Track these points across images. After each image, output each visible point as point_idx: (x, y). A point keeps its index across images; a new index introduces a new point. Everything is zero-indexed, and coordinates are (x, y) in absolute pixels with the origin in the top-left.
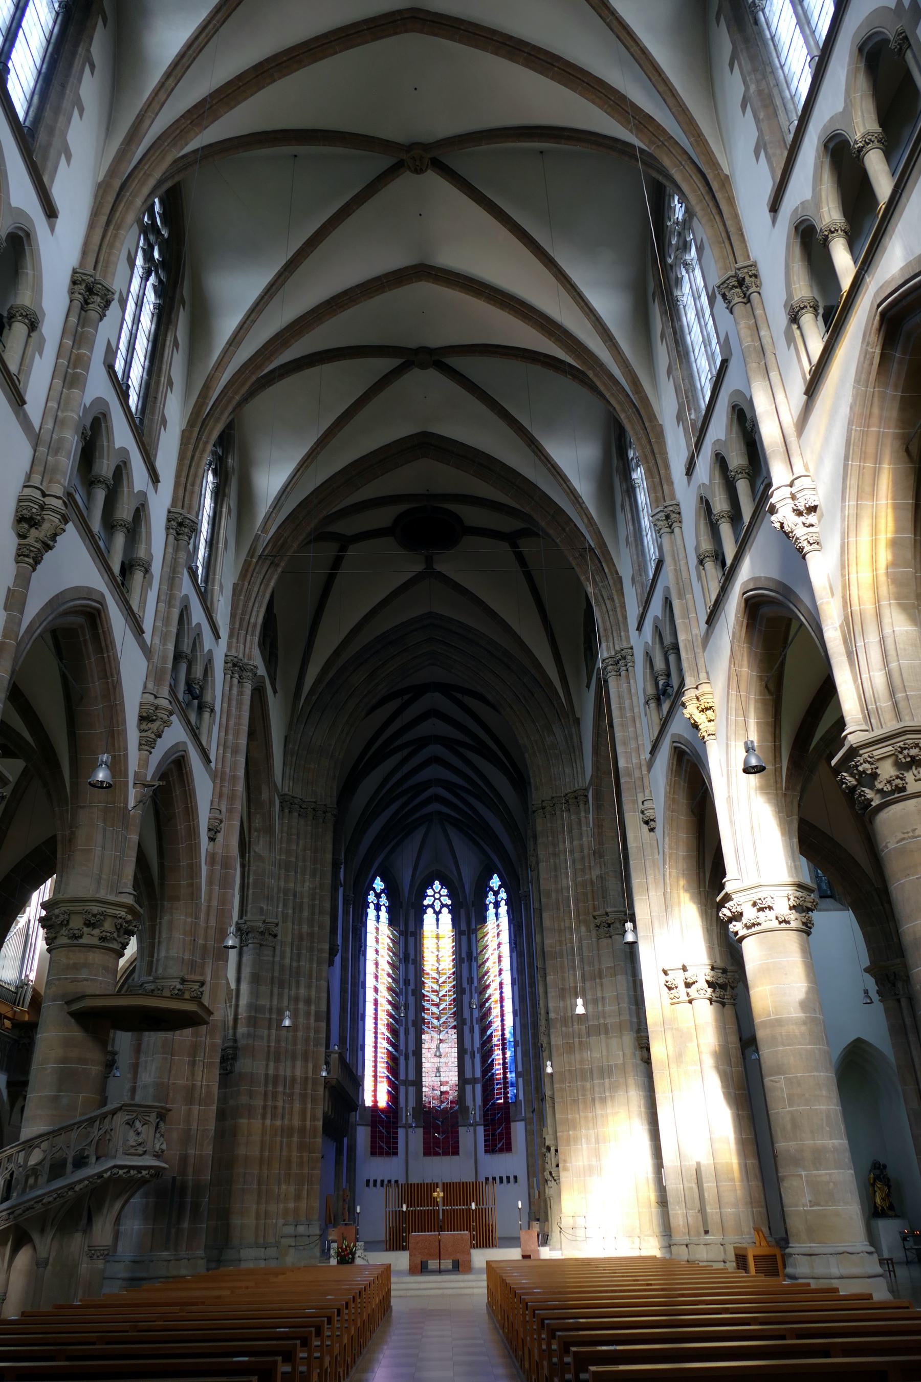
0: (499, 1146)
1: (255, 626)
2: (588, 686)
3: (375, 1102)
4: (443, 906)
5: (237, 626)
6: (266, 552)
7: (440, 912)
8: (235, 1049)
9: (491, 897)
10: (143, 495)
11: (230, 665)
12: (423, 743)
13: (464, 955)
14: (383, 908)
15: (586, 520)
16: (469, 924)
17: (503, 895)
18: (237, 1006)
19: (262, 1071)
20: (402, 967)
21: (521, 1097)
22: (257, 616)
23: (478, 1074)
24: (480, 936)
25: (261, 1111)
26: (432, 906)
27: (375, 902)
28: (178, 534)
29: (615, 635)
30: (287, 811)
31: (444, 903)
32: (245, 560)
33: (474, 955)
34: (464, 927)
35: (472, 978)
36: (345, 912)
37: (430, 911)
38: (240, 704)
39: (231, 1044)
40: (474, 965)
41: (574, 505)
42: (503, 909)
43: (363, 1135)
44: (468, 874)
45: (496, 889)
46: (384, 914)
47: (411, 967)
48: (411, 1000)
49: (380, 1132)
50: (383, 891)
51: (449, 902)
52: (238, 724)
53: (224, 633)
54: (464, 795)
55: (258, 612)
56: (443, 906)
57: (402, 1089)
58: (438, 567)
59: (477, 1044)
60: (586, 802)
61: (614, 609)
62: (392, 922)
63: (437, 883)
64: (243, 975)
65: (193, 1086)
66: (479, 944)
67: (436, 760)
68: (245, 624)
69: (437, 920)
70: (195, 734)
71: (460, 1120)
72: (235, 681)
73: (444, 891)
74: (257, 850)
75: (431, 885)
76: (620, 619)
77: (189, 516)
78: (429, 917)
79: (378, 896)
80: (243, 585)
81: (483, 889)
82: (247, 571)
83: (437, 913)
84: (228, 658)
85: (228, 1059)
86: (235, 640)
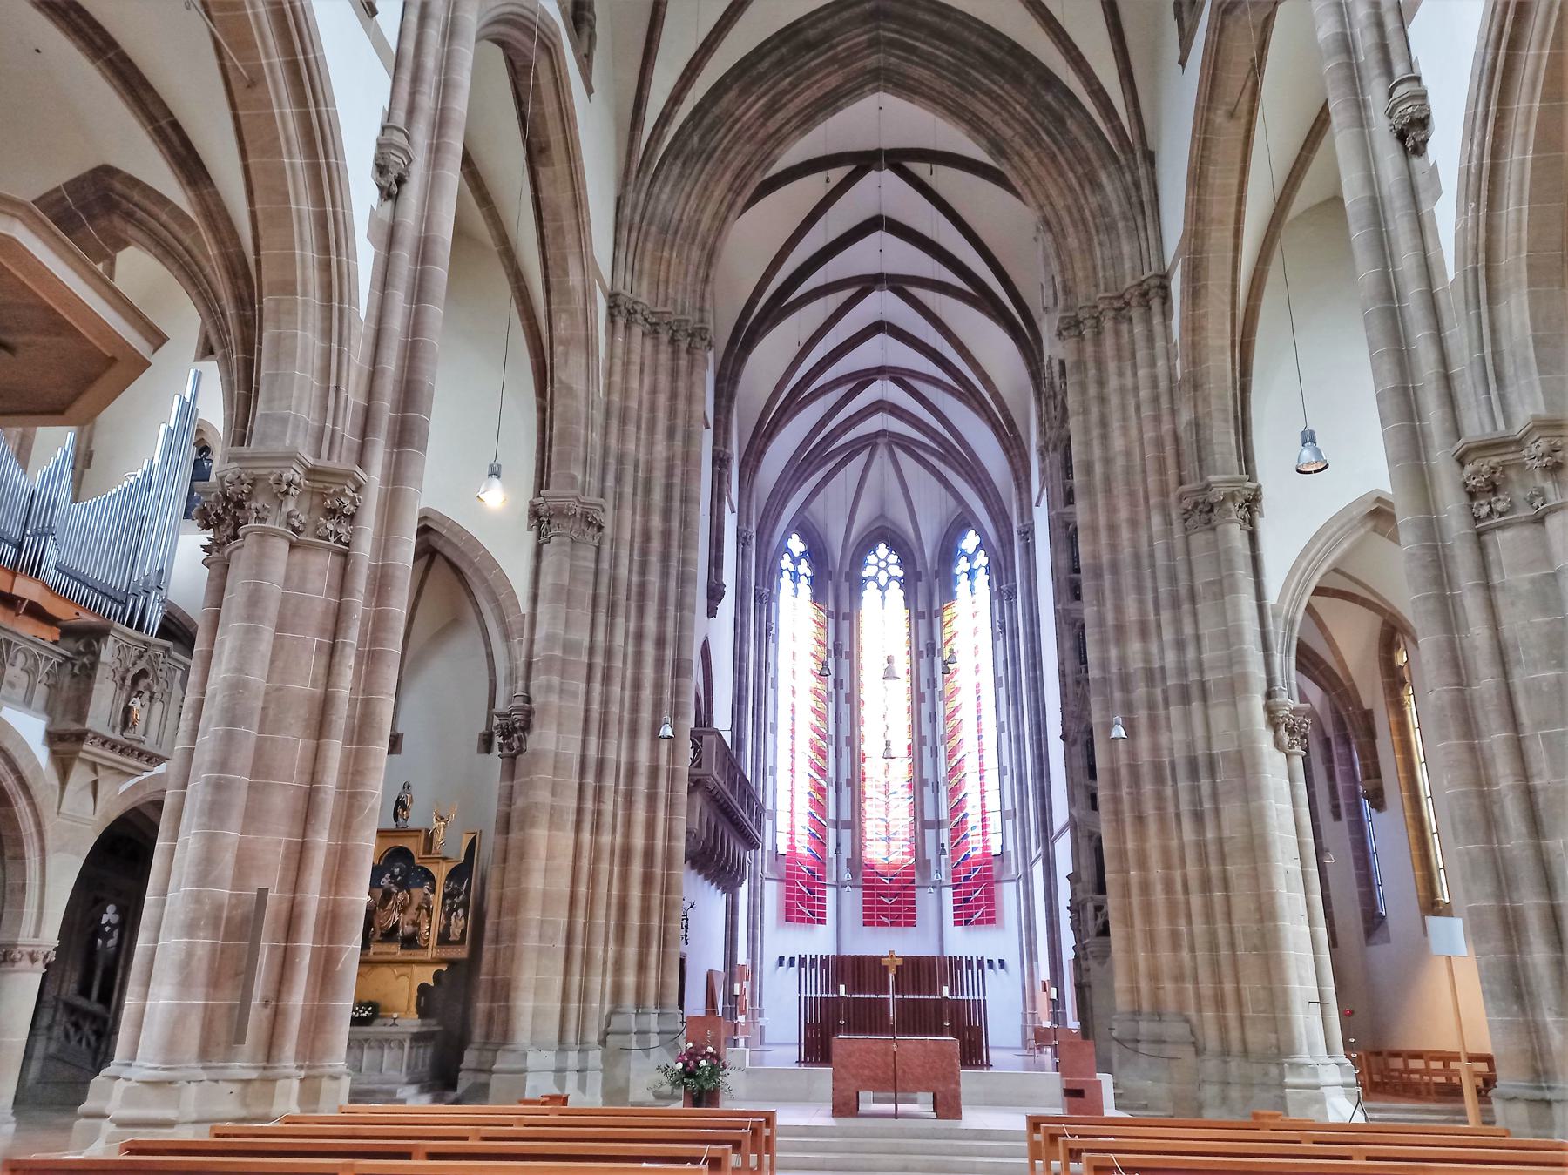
0: (976, 916)
2: (1182, 62)
3: (792, 847)
4: (890, 578)
7: (887, 587)
8: (529, 713)
9: (963, 565)
12: (864, 379)
13: (922, 647)
14: (803, 579)
17: (982, 559)
18: (531, 642)
19: (575, 751)
20: (831, 662)
21: (1010, 847)
23: (944, 814)
24: (946, 619)
26: (875, 578)
27: (792, 569)
30: (621, 321)
31: (893, 574)
33: (938, 646)
34: (922, 608)
35: (935, 680)
37: (871, 586)
39: (519, 703)
40: (938, 662)
42: (982, 579)
43: (772, 894)
45: (970, 551)
46: (805, 589)
47: (845, 663)
49: (800, 890)
51: (901, 573)
54: (922, 453)
57: (832, 832)
59: (943, 773)
60: (1166, 298)
62: (817, 598)
63: (882, 549)
64: (541, 592)
65: (550, 828)
66: (947, 630)
69: (883, 598)
71: (917, 878)
73: (893, 558)
78: (870, 594)
79: (795, 561)
81: (948, 553)
85: (515, 730)
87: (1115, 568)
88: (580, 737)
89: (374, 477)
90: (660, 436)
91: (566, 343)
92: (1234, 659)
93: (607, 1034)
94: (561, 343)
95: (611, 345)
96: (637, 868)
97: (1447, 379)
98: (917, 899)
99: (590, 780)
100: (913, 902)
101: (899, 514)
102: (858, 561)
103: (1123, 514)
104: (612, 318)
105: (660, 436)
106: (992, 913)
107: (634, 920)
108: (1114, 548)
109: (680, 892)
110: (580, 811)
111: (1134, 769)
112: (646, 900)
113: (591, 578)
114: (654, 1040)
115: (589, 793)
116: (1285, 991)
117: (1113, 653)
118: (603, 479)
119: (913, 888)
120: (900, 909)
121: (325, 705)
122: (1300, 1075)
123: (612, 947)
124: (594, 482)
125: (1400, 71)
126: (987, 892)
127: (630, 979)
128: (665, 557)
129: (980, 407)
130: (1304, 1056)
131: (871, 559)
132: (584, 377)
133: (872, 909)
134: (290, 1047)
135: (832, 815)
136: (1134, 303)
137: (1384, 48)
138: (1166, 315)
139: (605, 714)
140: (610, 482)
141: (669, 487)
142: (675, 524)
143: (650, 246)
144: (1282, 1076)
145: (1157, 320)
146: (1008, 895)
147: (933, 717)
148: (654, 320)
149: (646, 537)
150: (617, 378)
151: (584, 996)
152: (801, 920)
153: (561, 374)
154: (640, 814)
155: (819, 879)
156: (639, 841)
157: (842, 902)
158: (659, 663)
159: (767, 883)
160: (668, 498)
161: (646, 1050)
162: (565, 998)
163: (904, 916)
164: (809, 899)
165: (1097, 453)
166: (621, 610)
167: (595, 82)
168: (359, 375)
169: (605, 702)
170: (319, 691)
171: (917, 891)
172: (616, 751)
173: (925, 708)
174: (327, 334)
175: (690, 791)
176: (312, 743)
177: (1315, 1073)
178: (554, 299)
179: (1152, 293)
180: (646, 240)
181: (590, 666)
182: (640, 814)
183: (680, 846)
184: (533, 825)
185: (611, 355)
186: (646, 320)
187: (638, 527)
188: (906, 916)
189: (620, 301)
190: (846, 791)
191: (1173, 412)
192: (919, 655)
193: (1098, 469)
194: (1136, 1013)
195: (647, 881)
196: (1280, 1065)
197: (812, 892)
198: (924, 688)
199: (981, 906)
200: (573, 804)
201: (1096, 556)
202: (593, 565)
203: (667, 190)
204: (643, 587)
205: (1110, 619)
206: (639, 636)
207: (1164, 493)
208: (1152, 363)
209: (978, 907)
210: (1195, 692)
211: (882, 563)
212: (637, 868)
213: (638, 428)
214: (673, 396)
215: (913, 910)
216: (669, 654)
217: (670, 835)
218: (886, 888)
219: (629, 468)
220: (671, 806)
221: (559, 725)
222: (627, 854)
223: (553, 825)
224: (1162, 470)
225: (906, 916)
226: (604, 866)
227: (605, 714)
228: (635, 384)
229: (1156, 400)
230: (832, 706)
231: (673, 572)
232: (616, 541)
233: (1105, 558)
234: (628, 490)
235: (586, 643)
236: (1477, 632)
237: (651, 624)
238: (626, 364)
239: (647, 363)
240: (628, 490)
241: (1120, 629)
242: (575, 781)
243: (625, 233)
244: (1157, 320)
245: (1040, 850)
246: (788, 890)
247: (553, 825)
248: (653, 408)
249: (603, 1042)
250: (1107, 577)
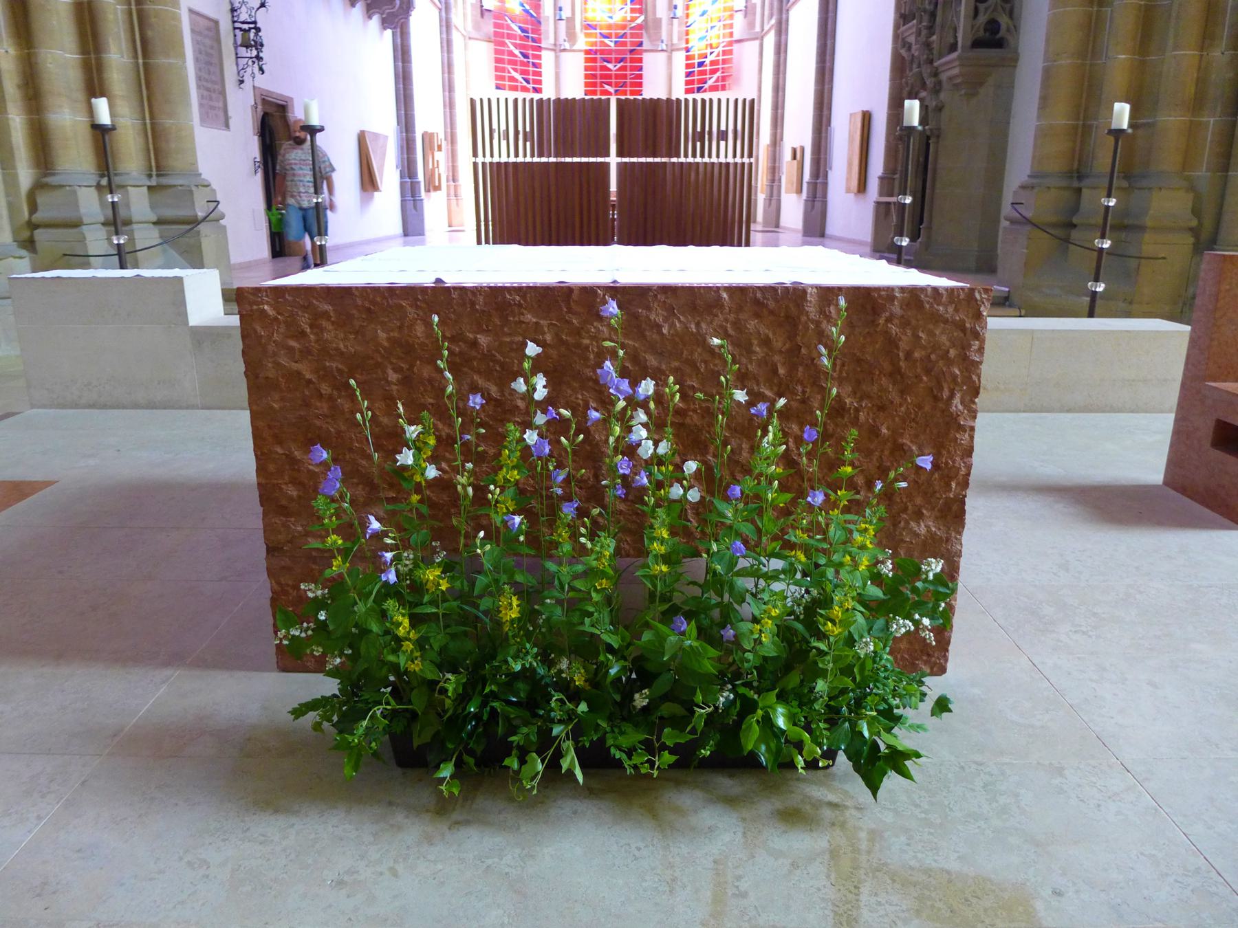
0: (710, 82)
49: (511, 53)
98: (644, 64)
100: (640, 69)
119: (641, 52)
120: (625, 76)
133: (594, 76)
155: (534, 40)
164: (523, 64)
171: (645, 56)
188: (633, 84)
197: (526, 56)
199: (717, 70)
209: (713, 72)
215: (640, 77)
218: (610, 52)
225: (633, 84)
245: (773, 21)
246: (497, 52)
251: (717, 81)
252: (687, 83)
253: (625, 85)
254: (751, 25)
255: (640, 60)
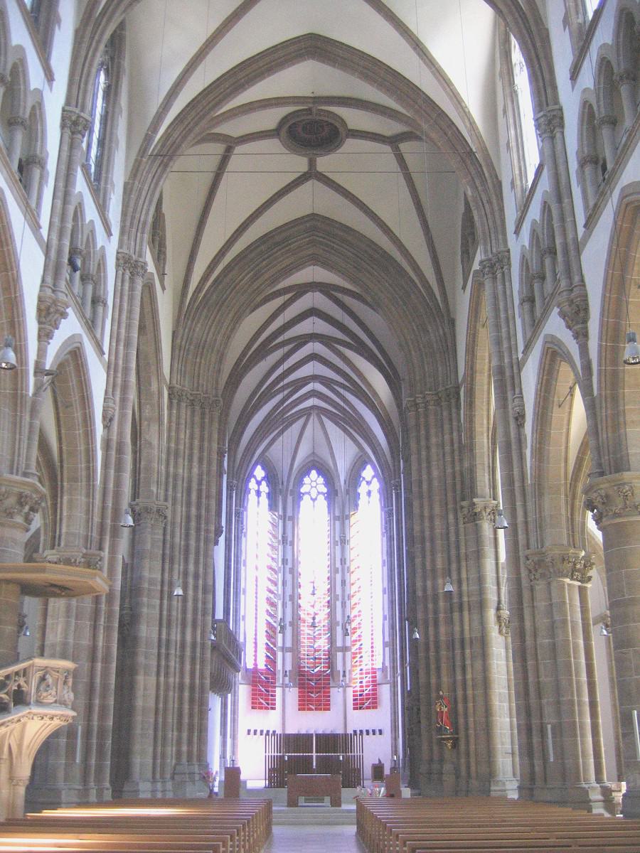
0: (366, 704)
1: (145, 223)
2: (464, 288)
3: (256, 665)
4: (319, 493)
5: (128, 224)
6: (156, 151)
7: (316, 499)
10: (39, 93)
11: (122, 262)
13: (337, 538)
15: (468, 125)
16: (343, 511)
17: (376, 485)
19: (155, 636)
20: (281, 547)
22: (147, 213)
25: (155, 669)
26: (309, 493)
27: (257, 489)
28: (73, 133)
29: (493, 238)
30: (175, 401)
31: (320, 491)
32: (136, 160)
36: (230, 497)
37: (306, 498)
38: (131, 298)
41: (457, 109)
42: (376, 496)
43: (243, 692)
44: (342, 466)
46: (264, 500)
47: (289, 548)
48: (289, 577)
49: (260, 690)
50: (263, 479)
52: (130, 318)
53: (116, 230)
54: (341, 391)
55: (148, 210)
56: (319, 493)
57: (280, 655)
58: (320, 168)
60: (458, 399)
61: (493, 213)
62: (273, 507)
63: (314, 473)
67: (313, 357)
68: (136, 222)
70: (91, 325)
72: (127, 277)
73: (321, 480)
74: (147, 437)
75: (308, 473)
76: (498, 222)
77: (82, 114)
78: (305, 503)
79: (259, 483)
80: (134, 184)
82: (137, 170)
83: (314, 500)
84: (119, 255)
86: (126, 238)
87: (432, 540)
88: (157, 628)
89: (106, 554)
90: (195, 464)
91: (149, 420)
92: (481, 591)
93: (174, 774)
94: (146, 420)
95: (170, 415)
96: (186, 694)
97: (526, 523)
98: (331, 694)
99: (163, 651)
100: (329, 697)
101: (324, 453)
102: (300, 483)
103: (437, 510)
104: (170, 399)
105: (195, 464)
106: (376, 703)
107: (186, 720)
108: (432, 528)
109: (208, 706)
110: (159, 666)
111: (437, 642)
112: (191, 709)
113: (161, 544)
114: (197, 777)
115: (163, 657)
116: (494, 749)
117: (429, 583)
118: (166, 490)
119: (329, 688)
121: (94, 649)
122: (497, 786)
123: (175, 733)
124: (162, 492)
125: (517, 391)
126: (373, 690)
127: (185, 748)
128: (198, 530)
129: (372, 407)
130: (501, 777)
131: (306, 480)
132: (157, 436)
134: (92, 778)
135: (280, 644)
136: (443, 400)
137: (513, 378)
138: (458, 407)
139: (169, 615)
140: (170, 492)
141: (200, 491)
142: (203, 512)
143: (190, 357)
144: (490, 786)
145: (454, 410)
146: (385, 692)
147: (343, 582)
148: (192, 398)
149: (188, 518)
150: (173, 434)
151: (163, 755)
152: (261, 708)
153: (145, 436)
154: (188, 667)
155: (272, 683)
156: (187, 680)
157: (286, 696)
158: (196, 587)
159: (241, 686)
160: (199, 497)
161: (193, 781)
162: (155, 758)
163: (324, 705)
164: (266, 695)
165: (425, 477)
166: (177, 560)
167: (166, 283)
168: (98, 508)
169: (169, 610)
170: (91, 643)
171: (332, 690)
172: (176, 636)
173: (339, 577)
174: (88, 495)
175: (212, 651)
176: (90, 664)
177: (504, 784)
178: (143, 397)
179: (451, 397)
180: (188, 354)
181: (162, 591)
182: (188, 667)
183: (208, 682)
184: (137, 674)
185: (170, 421)
186: (188, 398)
187: (184, 513)
188: (324, 705)
189: (175, 390)
190: (289, 630)
191: (461, 460)
192: (335, 543)
193: (425, 486)
194: (431, 761)
195: (192, 700)
196: (490, 782)
197: (267, 691)
198: (338, 565)
200: (154, 663)
201: (423, 532)
202: (161, 537)
203: (199, 325)
204: (187, 546)
205: (428, 567)
206: (186, 574)
207: (455, 502)
208: (451, 433)
209: (368, 699)
210: (466, 606)
211: (314, 483)
212: (186, 694)
213: (184, 459)
214: (202, 439)
215: (329, 701)
216: (201, 582)
217: (202, 677)
218: (312, 688)
219: (180, 483)
220: (203, 661)
221: (148, 622)
222: (181, 687)
223: (146, 674)
224: (454, 491)
225: (324, 705)
226: (171, 693)
227: (169, 615)
228: (182, 436)
229: (453, 452)
230: (280, 575)
231: (202, 537)
232: (173, 524)
233: (427, 533)
234: (179, 495)
235: (159, 579)
236: (528, 624)
237: (191, 567)
238: (178, 424)
239: (188, 420)
240: (179, 495)
241: (434, 571)
242: (155, 651)
243: (177, 352)
244: (454, 410)
246: (253, 690)
247: (146, 674)
248: (191, 448)
249: (173, 778)
250: (428, 544)
251: (369, 704)
252: (354, 704)
253: (320, 705)
254: (386, 676)
255: (329, 692)
